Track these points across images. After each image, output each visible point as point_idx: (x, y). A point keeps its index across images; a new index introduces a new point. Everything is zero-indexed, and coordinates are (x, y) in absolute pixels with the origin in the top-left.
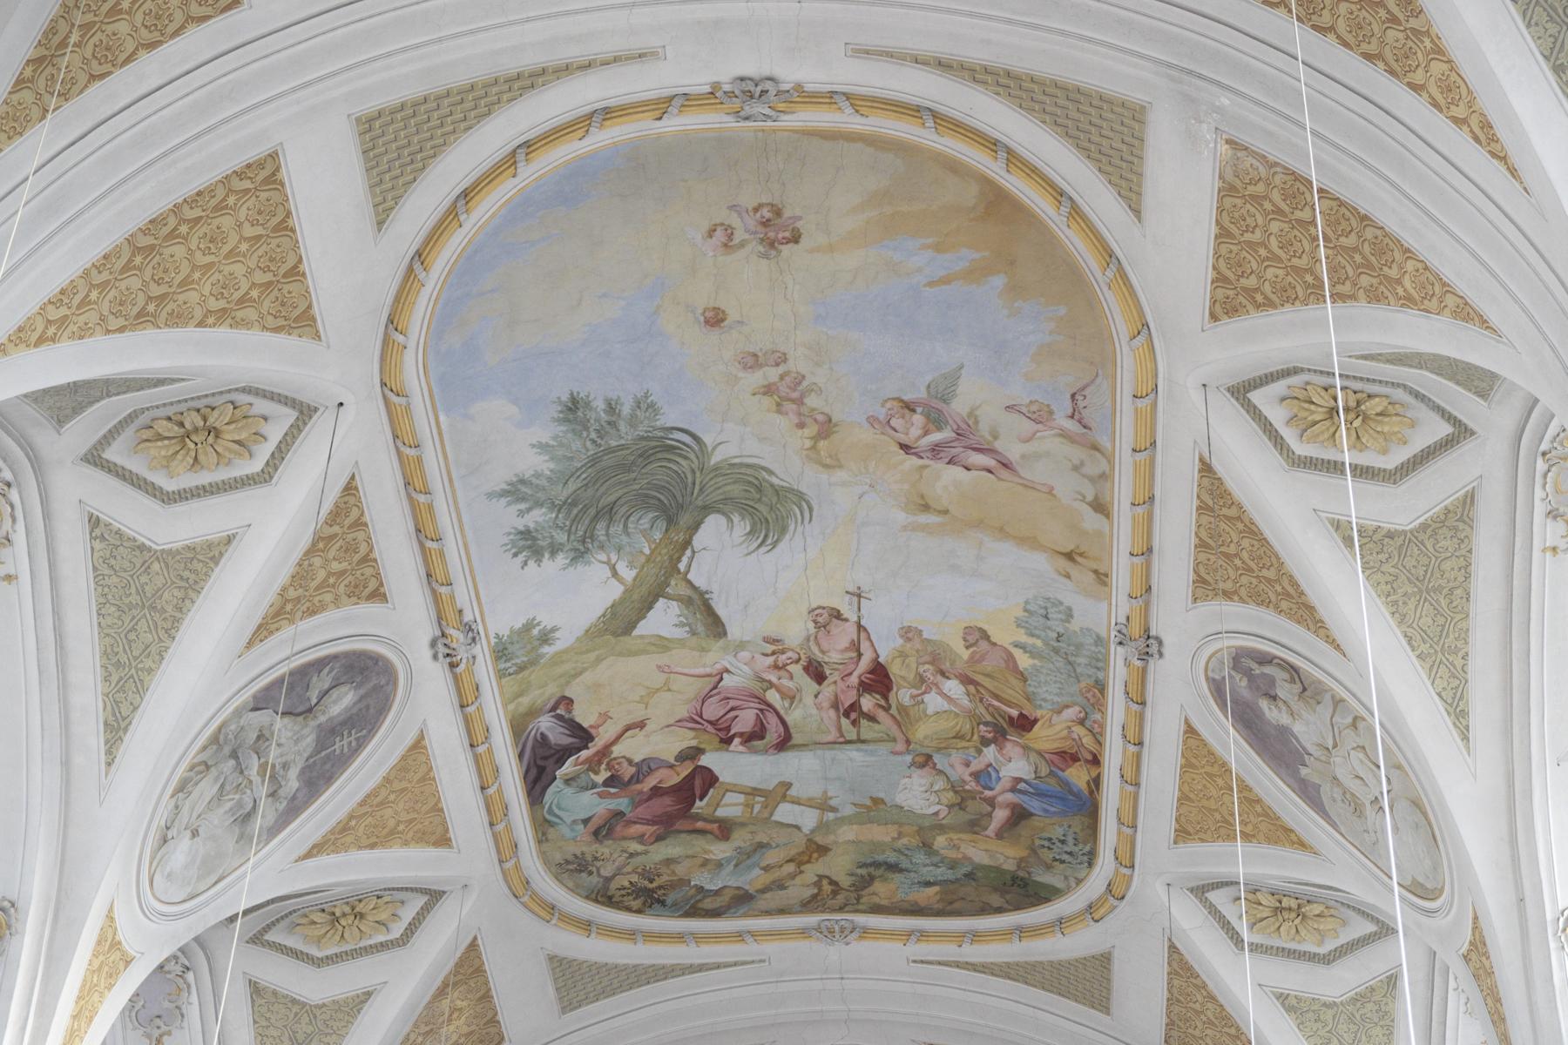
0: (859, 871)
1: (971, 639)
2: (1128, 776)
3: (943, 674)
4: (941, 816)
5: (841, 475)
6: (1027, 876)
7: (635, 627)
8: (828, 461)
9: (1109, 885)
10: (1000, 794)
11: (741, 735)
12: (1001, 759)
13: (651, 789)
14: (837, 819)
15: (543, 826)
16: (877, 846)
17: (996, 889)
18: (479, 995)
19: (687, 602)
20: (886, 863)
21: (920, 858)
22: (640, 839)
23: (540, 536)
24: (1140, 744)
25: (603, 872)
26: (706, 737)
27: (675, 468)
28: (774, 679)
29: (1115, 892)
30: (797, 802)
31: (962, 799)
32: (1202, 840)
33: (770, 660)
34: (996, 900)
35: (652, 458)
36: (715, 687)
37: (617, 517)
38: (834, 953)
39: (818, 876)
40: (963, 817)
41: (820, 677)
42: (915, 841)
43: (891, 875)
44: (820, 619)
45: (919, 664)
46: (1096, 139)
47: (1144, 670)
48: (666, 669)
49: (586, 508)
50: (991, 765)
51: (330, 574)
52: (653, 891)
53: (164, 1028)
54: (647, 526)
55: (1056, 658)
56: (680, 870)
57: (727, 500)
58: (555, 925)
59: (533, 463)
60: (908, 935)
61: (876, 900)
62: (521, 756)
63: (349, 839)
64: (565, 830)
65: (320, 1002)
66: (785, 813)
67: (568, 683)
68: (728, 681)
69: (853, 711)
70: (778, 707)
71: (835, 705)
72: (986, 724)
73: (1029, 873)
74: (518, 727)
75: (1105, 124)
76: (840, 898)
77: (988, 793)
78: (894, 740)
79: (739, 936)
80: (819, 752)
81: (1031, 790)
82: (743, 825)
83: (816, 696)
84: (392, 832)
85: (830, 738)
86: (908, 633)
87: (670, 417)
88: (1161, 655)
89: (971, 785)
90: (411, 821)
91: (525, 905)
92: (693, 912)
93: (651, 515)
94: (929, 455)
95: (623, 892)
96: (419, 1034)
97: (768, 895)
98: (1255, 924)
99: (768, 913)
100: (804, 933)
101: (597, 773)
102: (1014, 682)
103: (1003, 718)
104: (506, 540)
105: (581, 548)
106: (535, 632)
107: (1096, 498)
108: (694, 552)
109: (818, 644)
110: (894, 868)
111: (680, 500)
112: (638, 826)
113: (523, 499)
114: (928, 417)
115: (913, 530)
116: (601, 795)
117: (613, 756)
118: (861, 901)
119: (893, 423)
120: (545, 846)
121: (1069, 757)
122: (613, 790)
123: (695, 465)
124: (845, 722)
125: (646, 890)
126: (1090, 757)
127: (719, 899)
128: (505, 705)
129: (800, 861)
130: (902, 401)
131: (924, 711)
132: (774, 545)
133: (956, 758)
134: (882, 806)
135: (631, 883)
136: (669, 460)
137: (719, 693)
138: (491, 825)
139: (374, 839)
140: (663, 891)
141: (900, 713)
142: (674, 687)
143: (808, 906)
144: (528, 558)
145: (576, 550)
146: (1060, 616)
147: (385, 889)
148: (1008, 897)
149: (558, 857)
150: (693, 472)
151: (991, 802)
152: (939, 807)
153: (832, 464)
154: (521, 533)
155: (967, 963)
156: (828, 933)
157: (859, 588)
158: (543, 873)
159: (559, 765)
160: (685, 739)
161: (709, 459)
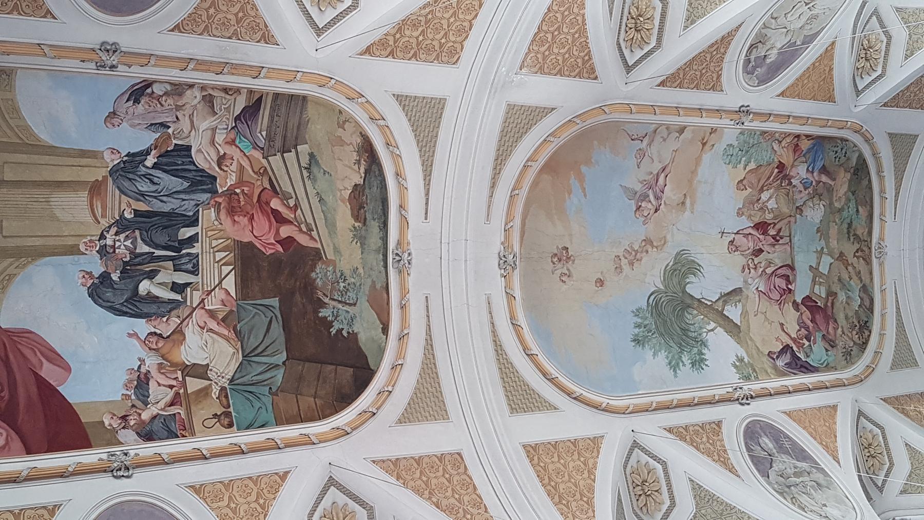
0: (852, 240)
3: (759, 200)
4: (824, 203)
5: (669, 237)
6: (853, 169)
8: (663, 242)
10: (814, 177)
11: (787, 285)
15: (828, 368)
19: (725, 302)
21: (845, 214)
22: (835, 329)
28: (761, 269)
31: (816, 195)
33: (752, 271)
34: (865, 182)
36: (765, 294)
37: (687, 328)
40: (825, 193)
42: (837, 215)
43: (853, 227)
44: (734, 250)
49: (683, 340)
50: (801, 182)
51: (708, 442)
52: (860, 326)
54: (691, 316)
59: (662, 357)
62: (795, 374)
63: (831, 445)
64: (830, 359)
66: (824, 269)
67: (762, 353)
70: (774, 269)
71: (774, 245)
72: (781, 183)
74: (781, 374)
76: (865, 249)
77: (814, 183)
78: (790, 222)
82: (829, 286)
83: (769, 253)
84: (830, 428)
85: (789, 249)
86: (740, 213)
87: (644, 305)
91: (866, 378)
92: (871, 310)
93: (686, 314)
95: (861, 337)
97: (863, 278)
99: (872, 279)
100: (881, 264)
101: (804, 344)
102: (762, 170)
104: (696, 372)
110: (850, 225)
112: (829, 329)
113: (678, 364)
114: (643, 201)
115: (693, 209)
119: (646, 215)
120: (838, 367)
122: (812, 338)
124: (780, 242)
129: (847, 265)
130: (636, 211)
131: (777, 208)
132: (700, 266)
133: (797, 196)
139: (832, 436)
143: (868, 262)
144: (704, 364)
145: (701, 345)
147: (857, 434)
149: (844, 363)
150: (667, 296)
154: (693, 366)
155: (895, 196)
160: (789, 307)
161: (661, 289)
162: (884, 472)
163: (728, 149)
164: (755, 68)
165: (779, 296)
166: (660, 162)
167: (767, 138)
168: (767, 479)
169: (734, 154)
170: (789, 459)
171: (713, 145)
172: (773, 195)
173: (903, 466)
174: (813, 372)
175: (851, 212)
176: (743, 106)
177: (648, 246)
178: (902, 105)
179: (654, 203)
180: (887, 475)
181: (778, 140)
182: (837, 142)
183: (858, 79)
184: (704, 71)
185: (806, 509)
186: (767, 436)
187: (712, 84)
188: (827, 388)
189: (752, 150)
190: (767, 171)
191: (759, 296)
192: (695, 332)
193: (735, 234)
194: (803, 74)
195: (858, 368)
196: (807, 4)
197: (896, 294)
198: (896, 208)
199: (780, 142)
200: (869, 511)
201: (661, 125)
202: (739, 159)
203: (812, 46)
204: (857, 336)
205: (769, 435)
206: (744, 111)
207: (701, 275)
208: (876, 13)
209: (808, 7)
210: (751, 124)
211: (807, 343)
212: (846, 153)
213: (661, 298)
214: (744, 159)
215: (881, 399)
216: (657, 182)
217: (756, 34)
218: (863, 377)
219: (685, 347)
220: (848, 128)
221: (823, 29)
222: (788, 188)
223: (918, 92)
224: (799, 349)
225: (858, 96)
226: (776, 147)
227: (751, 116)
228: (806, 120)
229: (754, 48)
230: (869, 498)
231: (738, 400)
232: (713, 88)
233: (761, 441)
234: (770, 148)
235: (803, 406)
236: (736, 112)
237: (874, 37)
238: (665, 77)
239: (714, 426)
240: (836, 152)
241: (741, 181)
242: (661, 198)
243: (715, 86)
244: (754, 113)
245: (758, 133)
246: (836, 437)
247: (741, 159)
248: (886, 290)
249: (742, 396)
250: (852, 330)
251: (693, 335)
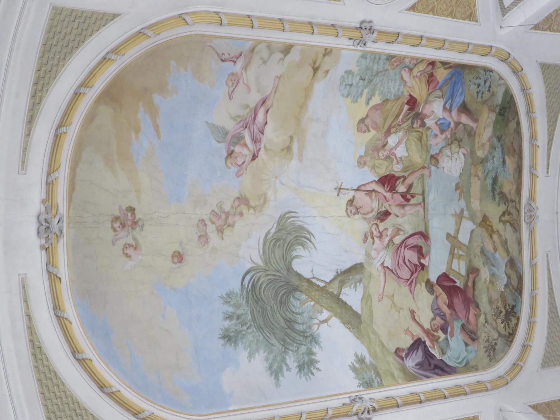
0: (497, 199)
1: (364, 128)
2: (440, 45)
3: (384, 146)
4: (465, 152)
5: (270, 194)
8: (262, 200)
9: (502, 61)
10: (451, 117)
11: (419, 259)
12: (432, 117)
13: (449, 309)
14: (468, 210)
16: (483, 189)
17: (506, 125)
19: (342, 283)
20: (492, 185)
21: (489, 165)
22: (477, 316)
23: (302, 360)
24: (422, 37)
27: (265, 285)
28: (387, 239)
29: (505, 59)
30: (458, 231)
32: (475, 6)
33: (377, 240)
34: (512, 125)
35: (259, 297)
36: (392, 271)
39: (499, 222)
40: (466, 139)
41: (386, 214)
42: (480, 168)
43: (499, 183)
44: (353, 211)
45: (379, 159)
46: (72, 37)
47: (380, 32)
48: (381, 297)
49: (287, 335)
52: (507, 311)
54: (298, 302)
56: (495, 296)
57: (284, 258)
58: (524, 364)
60: (533, 176)
61: (513, 192)
62: (428, 377)
64: (471, 356)
66: (464, 237)
67: (387, 350)
68: (388, 264)
69: (406, 197)
71: (403, 206)
72: (413, 123)
73: (497, 106)
74: (411, 378)
75: (64, 31)
76: (513, 211)
77: (452, 125)
78: (422, 175)
79: (533, 266)
80: (429, 217)
82: (470, 261)
83: (398, 216)
85: (421, 210)
86: (361, 163)
87: (235, 286)
88: (370, 22)
89: (448, 134)
91: (512, 379)
92: (519, 290)
93: (292, 299)
94: (258, 144)
95: (507, 327)
97: (510, 250)
99: (520, 251)
100: (531, 232)
101: (439, 338)
102: (389, 106)
103: (409, 113)
104: (304, 379)
105: (310, 338)
106: (357, 366)
107: (281, 52)
108: (314, 278)
109: (368, 213)
110: (495, 180)
111: (283, 283)
112: (470, 317)
113: (280, 368)
114: (236, 144)
116: (452, 336)
117: (430, 328)
118: (514, 199)
119: (240, 163)
121: (430, 79)
122: (449, 330)
123: (264, 274)
124: (412, 201)
127: (512, 276)
128: (399, 384)
129: (491, 232)
130: (227, 158)
131: (406, 157)
132: (310, 233)
133: (432, 141)
134: (460, 185)
135: (502, 323)
136: (260, 288)
138: (466, 394)
140: (507, 306)
141: (407, 171)
142: (391, 294)
143: (516, 229)
144: (314, 367)
148: (511, 118)
149: (486, 360)
150: (267, 275)
151: (457, 124)
154: (300, 370)
155: (548, 144)
156: (532, 218)
157: (335, 189)
158: (494, 369)
159: (434, 358)
160: (421, 289)
165: (410, 273)
167: (395, 64)
171: (327, 72)
175: (496, 163)
182: (479, 73)
199: (411, 70)
201: (260, 42)
202: (360, 91)
211: (442, 336)
212: (490, 87)
213: (259, 278)
214: (366, 91)
216: (255, 119)
222: (421, 130)
224: (433, 345)
227: (375, 34)
234: (398, 78)
240: (479, 86)
241: (362, 121)
245: (383, 57)
247: (363, 91)
250: (497, 318)
251: (300, 328)
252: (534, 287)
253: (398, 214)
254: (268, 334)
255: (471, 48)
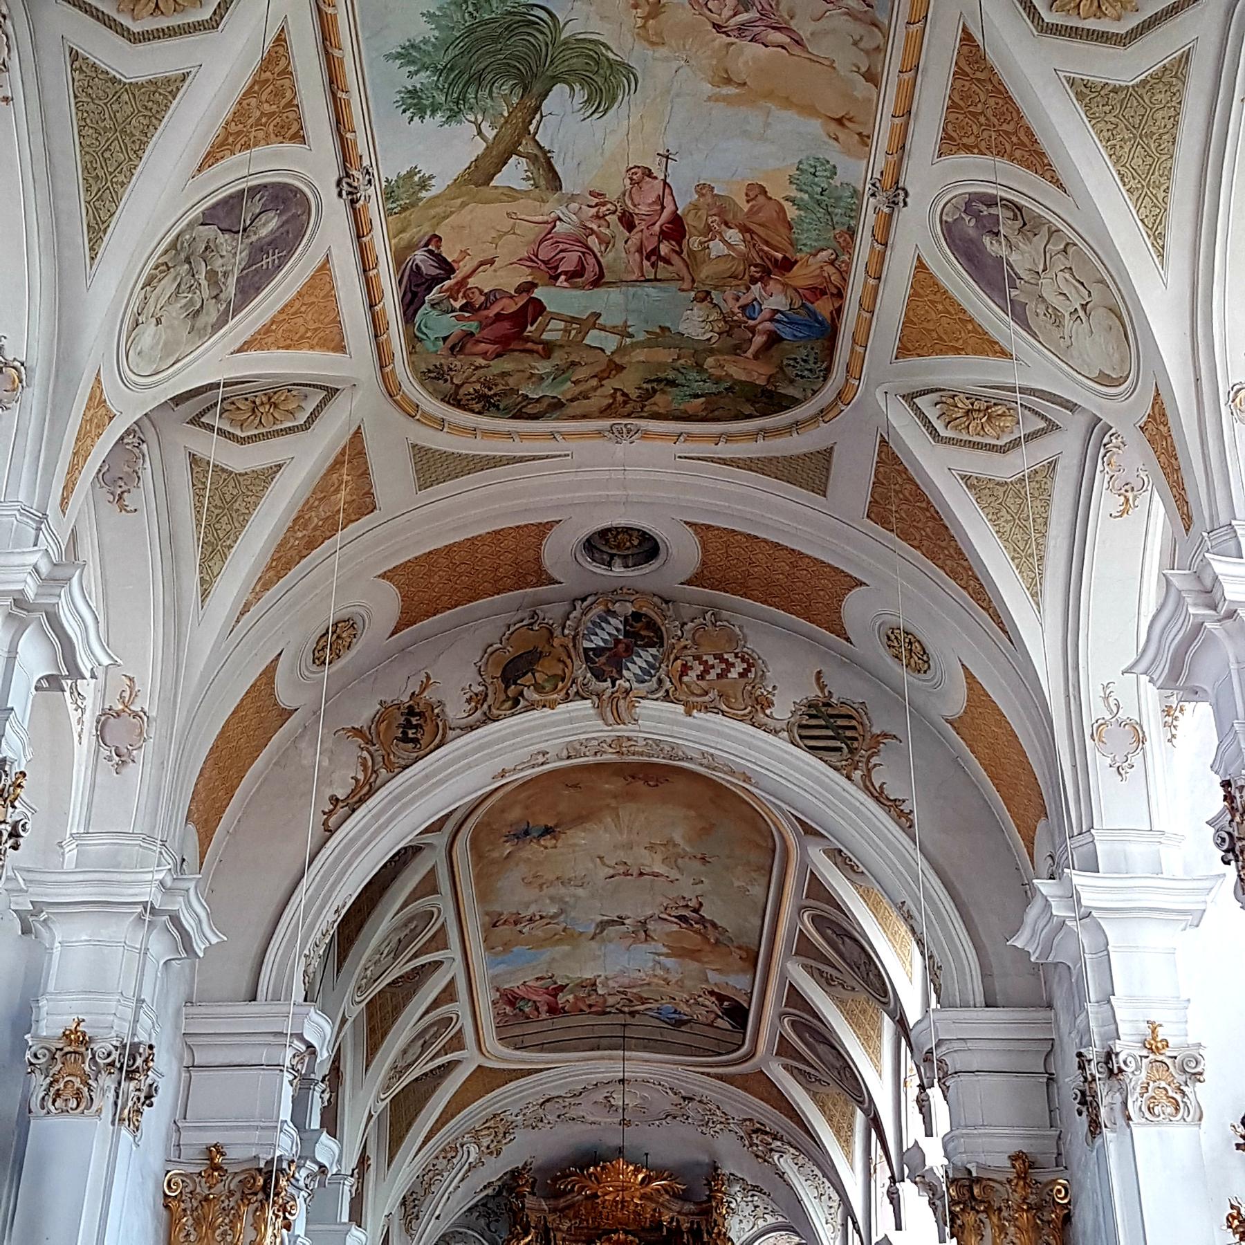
0: (645, 386)
1: (752, 195)
3: (726, 224)
4: (713, 341)
5: (663, 51)
7: (492, 179)
8: (654, 39)
11: (565, 273)
13: (495, 315)
14: (632, 344)
15: (413, 340)
16: (661, 366)
18: (360, 471)
19: (533, 159)
20: (666, 379)
21: (693, 375)
22: (484, 355)
23: (424, 96)
25: (455, 381)
26: (539, 273)
27: (532, 40)
28: (595, 227)
30: (603, 329)
31: (730, 326)
32: (919, 355)
34: (748, 409)
35: (516, 31)
36: (549, 233)
37: (484, 83)
38: (621, 450)
40: (732, 342)
44: (635, 177)
45: (708, 216)
48: (513, 216)
49: (461, 73)
50: (756, 299)
52: (491, 397)
53: (125, 488)
55: (818, 209)
57: (572, 71)
59: (424, 31)
61: (655, 408)
62: (400, 282)
63: (270, 340)
64: (429, 344)
65: (243, 471)
66: (593, 338)
67: (438, 224)
69: (653, 255)
70: (596, 250)
71: (640, 250)
72: (756, 266)
73: (776, 387)
74: (399, 257)
76: (629, 407)
77: (751, 323)
78: (682, 279)
80: (624, 289)
81: (785, 319)
82: (561, 346)
83: (626, 242)
84: (302, 337)
85: (634, 278)
86: (703, 189)
89: (740, 316)
90: (316, 330)
92: (519, 416)
94: (736, 33)
95: (469, 397)
96: (316, 499)
98: (949, 423)
99: (574, 417)
100: (600, 433)
101: (456, 300)
102: (783, 231)
103: (770, 260)
105: (455, 108)
108: (542, 117)
110: (672, 383)
111: (535, 69)
113: (413, 63)
115: (717, 100)
118: (645, 409)
120: (414, 357)
121: (818, 292)
122: (467, 315)
123: (549, 41)
124: (645, 262)
125: (485, 396)
126: (835, 291)
129: (601, 377)
132: (606, 111)
133: (729, 294)
134: (667, 334)
136: (529, 34)
137: (552, 238)
139: (289, 342)
143: (605, 412)
145: (451, 110)
146: (825, 174)
147: (294, 384)
150: (547, 45)
151: (753, 330)
152: (712, 334)
153: (656, 42)
154: (409, 92)
155: (719, 458)
157: (668, 151)
160: (524, 276)
161: (560, 33)
162: (227, 428)
163: (827, 166)
164: (977, 215)
166: (812, 34)
167: (841, 240)
168: (201, 221)
169: (816, 179)
170: (240, 264)
171: (836, 139)
172: (734, 250)
173: (242, 459)
174: (405, 315)
176: (906, 194)
177: (647, 9)
178: (881, 469)
179: (733, 21)
180: (221, 432)
181: (836, 259)
183: (935, 397)
184: (982, 120)
185: (148, 288)
186: (282, 226)
187: (954, 135)
188: (376, 336)
189: (821, 212)
190: (779, 238)
191: (546, 222)
192: (476, 98)
193: (665, 181)
194: (953, 302)
195: (413, 390)
196: (1084, 306)
197: (547, 457)
198: (699, 459)
199: (832, 263)
200: (155, 398)
201: (886, 36)
202: (805, 188)
203: (1009, 319)
204: (471, 390)
205: (285, 228)
206: (896, 195)
207: (588, 114)
208: (1052, 427)
209: (1079, 309)
210: (871, 210)
211: (457, 305)
212: (802, 377)
213: (542, 33)
215: (359, 427)
216: (773, 28)
217: (1040, 216)
218: (398, 397)
219: (447, 78)
220: (847, 380)
221: (1034, 336)
222: (746, 277)
223: (901, 496)
224: (446, 291)
225: (903, 397)
226: (824, 255)
227: (886, 210)
228: (869, 306)
229: (1015, 215)
230: (178, 400)
231: (348, 175)
232: (947, 138)
233: (271, 214)
234: (821, 244)
235: (342, 294)
236: (897, 183)
237: (1008, 424)
238: (981, 44)
239: (295, 128)
240: (805, 361)
241: (763, 191)
242: (740, 36)
243: (951, 142)
244: (891, 215)
245: (853, 223)
246: (288, 347)
247: (806, 192)
248: (553, 442)
249: (355, 184)
250: (482, 383)
251: (471, 96)
252: (523, 436)
253: (629, 242)
254: (461, 45)
255: (860, 350)
